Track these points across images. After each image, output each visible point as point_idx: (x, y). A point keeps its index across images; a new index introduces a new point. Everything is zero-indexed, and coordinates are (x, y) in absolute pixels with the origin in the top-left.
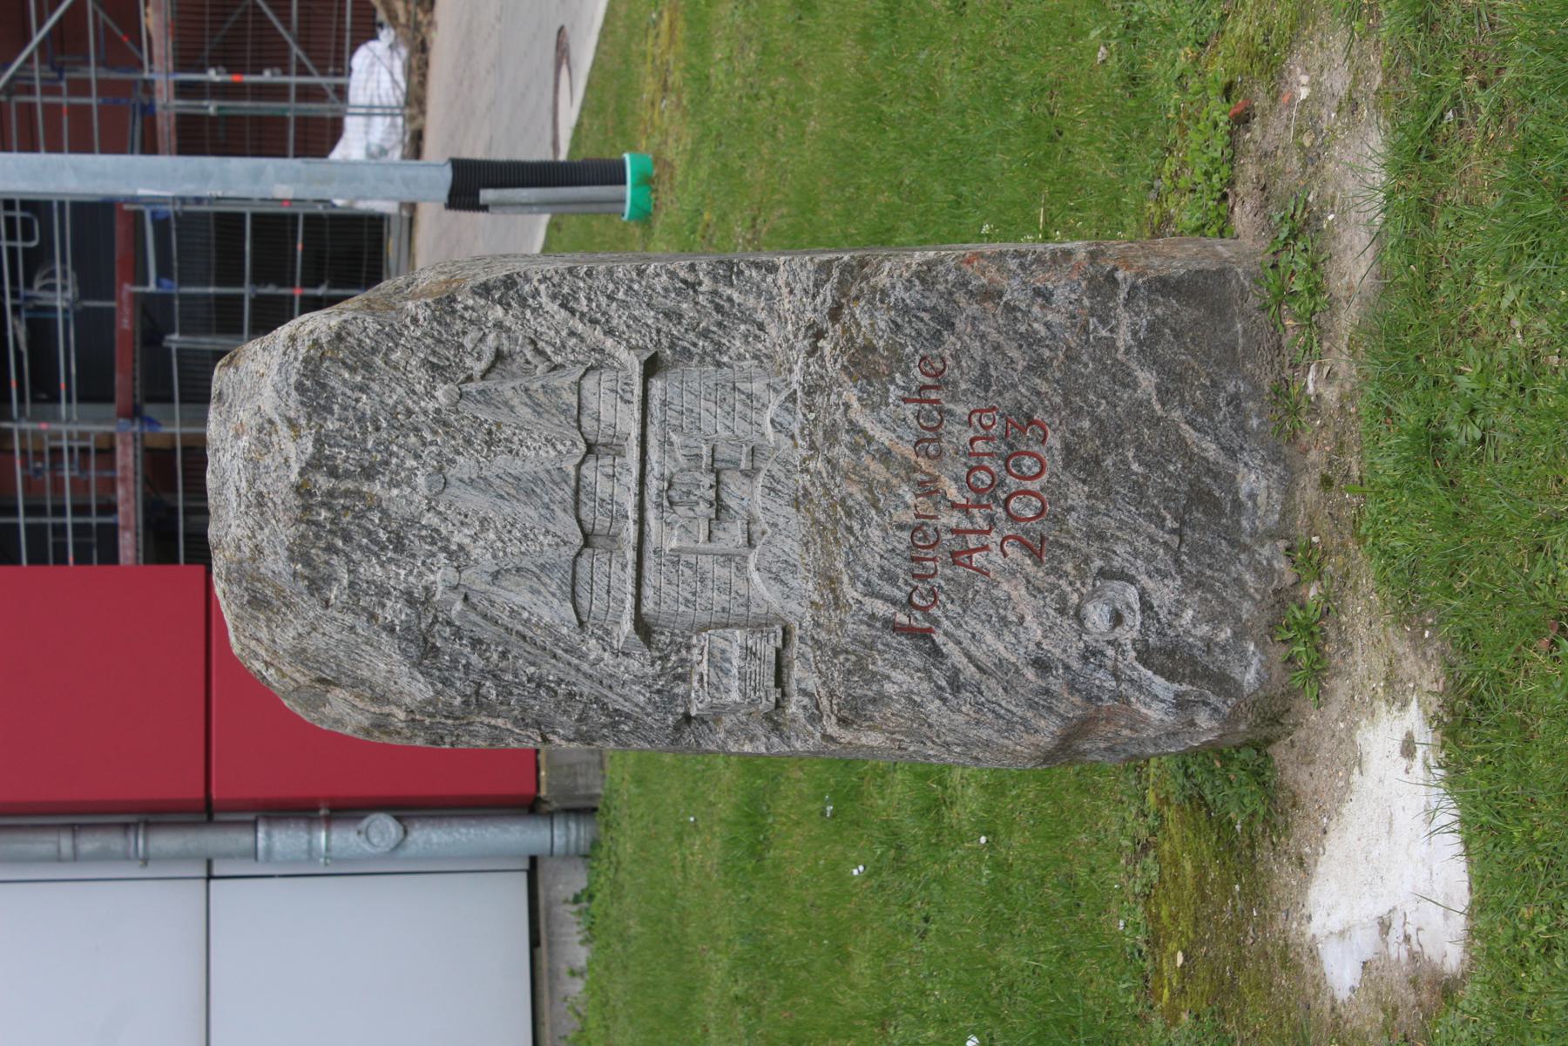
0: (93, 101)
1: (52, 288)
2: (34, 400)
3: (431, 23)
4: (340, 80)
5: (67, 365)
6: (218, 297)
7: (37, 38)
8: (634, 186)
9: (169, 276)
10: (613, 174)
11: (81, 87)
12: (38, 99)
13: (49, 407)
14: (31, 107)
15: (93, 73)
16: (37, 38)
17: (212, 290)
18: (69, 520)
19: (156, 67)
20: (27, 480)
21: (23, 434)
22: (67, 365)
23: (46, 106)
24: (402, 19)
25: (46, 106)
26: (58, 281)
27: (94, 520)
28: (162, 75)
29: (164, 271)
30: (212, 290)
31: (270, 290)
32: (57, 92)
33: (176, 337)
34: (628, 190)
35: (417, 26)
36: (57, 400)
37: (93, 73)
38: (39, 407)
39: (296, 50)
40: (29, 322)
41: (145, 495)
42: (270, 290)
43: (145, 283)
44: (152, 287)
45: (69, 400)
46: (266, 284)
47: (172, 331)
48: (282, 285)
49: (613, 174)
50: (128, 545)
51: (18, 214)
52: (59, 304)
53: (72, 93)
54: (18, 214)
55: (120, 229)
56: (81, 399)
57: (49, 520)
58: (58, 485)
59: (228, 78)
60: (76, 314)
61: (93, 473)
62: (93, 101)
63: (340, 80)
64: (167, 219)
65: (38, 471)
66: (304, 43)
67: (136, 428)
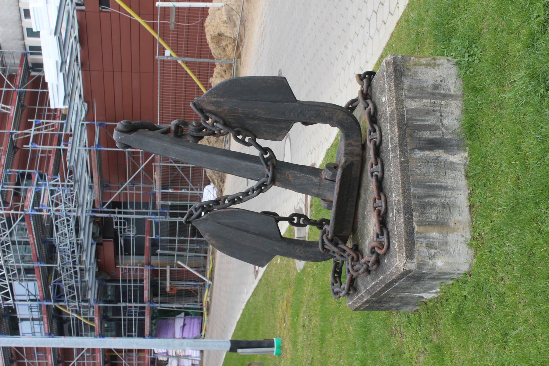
0: (141, 192)
1: (130, 231)
2: (125, 255)
3: (223, 186)
4: (201, 192)
5: (133, 249)
6: (170, 239)
7: (128, 181)
8: (277, 348)
9: (158, 235)
10: (270, 344)
11: (138, 189)
12: (128, 192)
13: (128, 256)
14: (126, 193)
15: (141, 185)
16: (128, 181)
17: (168, 238)
18: (132, 284)
19: (157, 188)
20: (122, 275)
21: (122, 268)
22: (133, 249)
23: (130, 193)
24: (216, 184)
25: (130, 193)
26: (131, 229)
27: (138, 284)
28: (158, 190)
29: (157, 233)
30: (168, 238)
31: (182, 238)
32: (133, 190)
33: (159, 250)
34: (275, 349)
35: (220, 186)
36: (130, 255)
37: (141, 185)
38: (126, 256)
39: (190, 184)
40: (124, 240)
41: (151, 278)
42: (182, 238)
43: (152, 236)
44: (154, 237)
45: (133, 255)
46: (182, 236)
47: (158, 249)
48: (185, 237)
49: (270, 344)
50: (146, 294)
51: (122, 221)
52: (132, 235)
53: (136, 190)
54: (122, 221)
55: (147, 224)
56: (136, 255)
57: (127, 284)
58: (130, 275)
59: (174, 191)
60: (136, 238)
61: (138, 273)
62: (141, 192)
63: (201, 192)
64: (158, 223)
65: (125, 273)
66: (192, 183)
67: (149, 268)
